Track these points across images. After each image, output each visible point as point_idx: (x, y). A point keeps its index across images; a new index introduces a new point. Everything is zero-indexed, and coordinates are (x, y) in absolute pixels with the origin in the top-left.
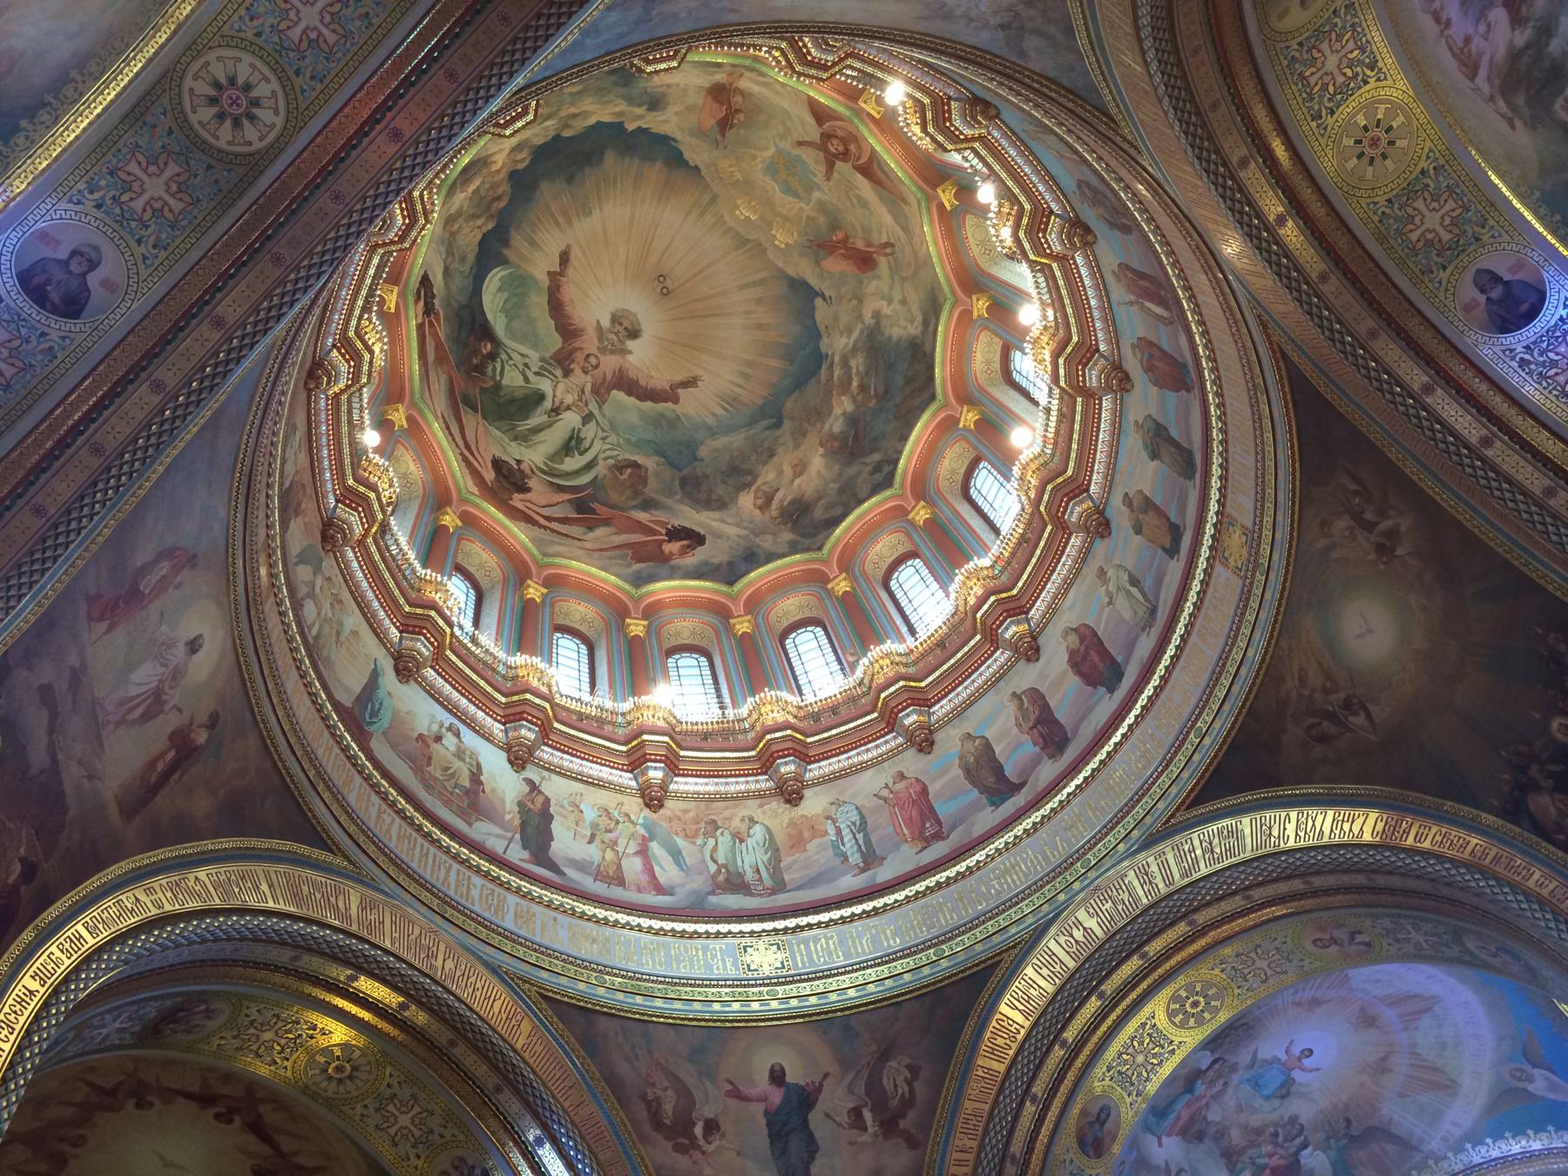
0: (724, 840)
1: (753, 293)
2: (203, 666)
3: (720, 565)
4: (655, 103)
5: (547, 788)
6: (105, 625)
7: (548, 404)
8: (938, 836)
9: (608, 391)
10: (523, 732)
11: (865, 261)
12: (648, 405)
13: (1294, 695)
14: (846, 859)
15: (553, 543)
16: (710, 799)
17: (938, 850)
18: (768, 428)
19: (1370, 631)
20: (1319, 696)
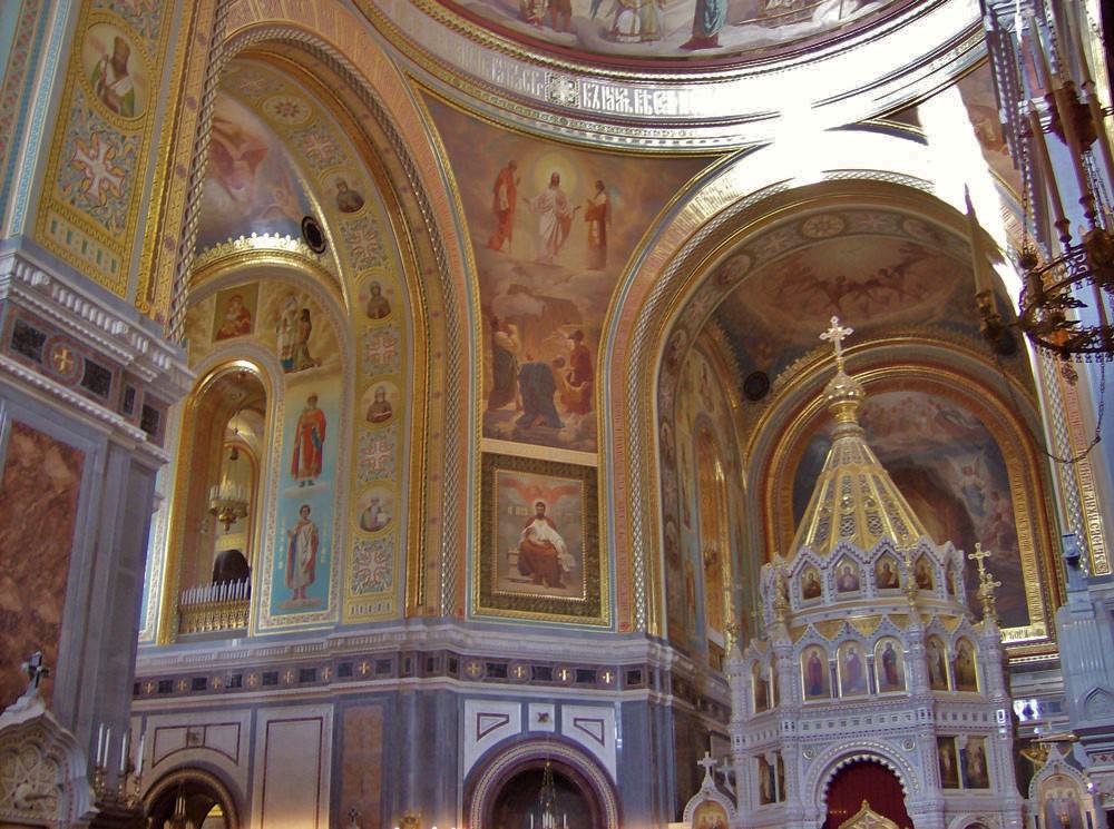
2: (568, 182)
6: (506, 241)
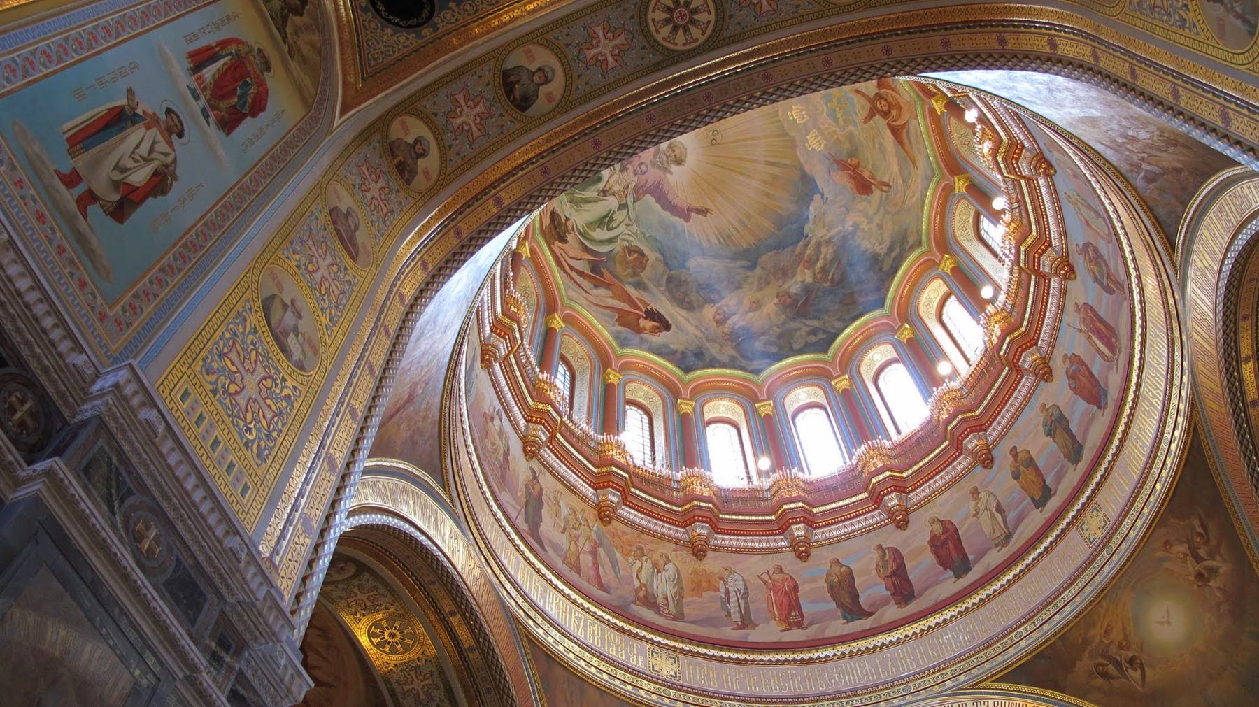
0: (647, 566)
1: (776, 171)
3: (674, 353)
5: (541, 479)
7: (601, 186)
8: (799, 625)
10: (540, 433)
11: (864, 187)
13: (1097, 640)
14: (729, 615)
16: (642, 530)
17: (796, 635)
18: (743, 267)
19: (1169, 623)
20: (1113, 648)
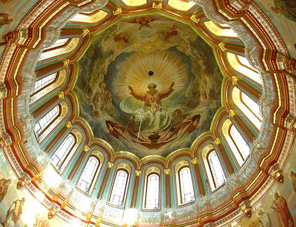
1: (166, 58)
4: (112, 53)
9: (160, 101)
11: (175, 33)
12: (170, 96)
15: (171, 145)
